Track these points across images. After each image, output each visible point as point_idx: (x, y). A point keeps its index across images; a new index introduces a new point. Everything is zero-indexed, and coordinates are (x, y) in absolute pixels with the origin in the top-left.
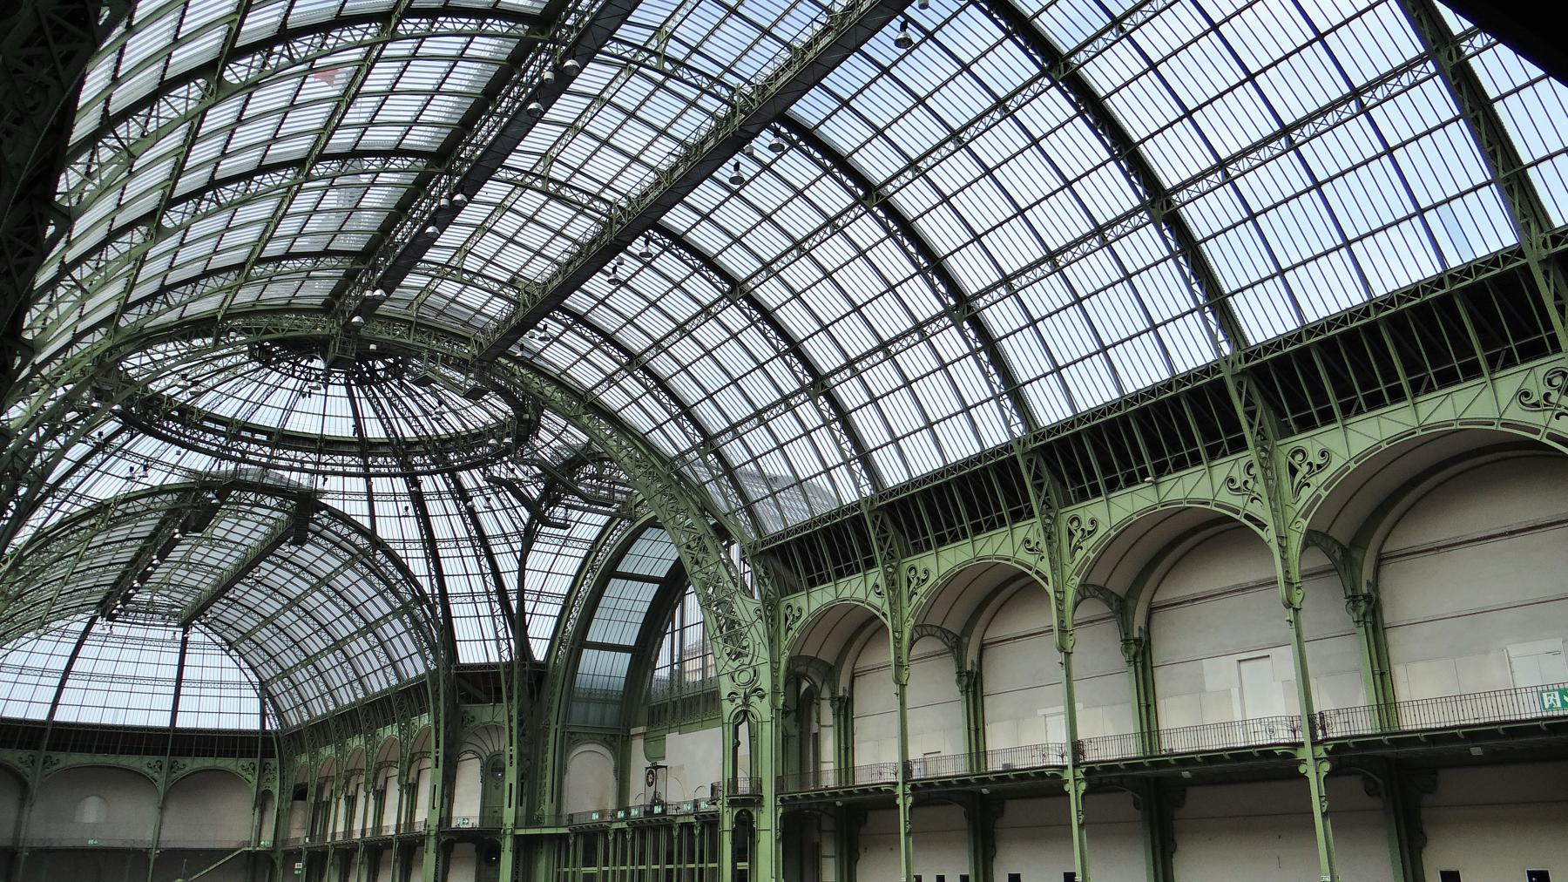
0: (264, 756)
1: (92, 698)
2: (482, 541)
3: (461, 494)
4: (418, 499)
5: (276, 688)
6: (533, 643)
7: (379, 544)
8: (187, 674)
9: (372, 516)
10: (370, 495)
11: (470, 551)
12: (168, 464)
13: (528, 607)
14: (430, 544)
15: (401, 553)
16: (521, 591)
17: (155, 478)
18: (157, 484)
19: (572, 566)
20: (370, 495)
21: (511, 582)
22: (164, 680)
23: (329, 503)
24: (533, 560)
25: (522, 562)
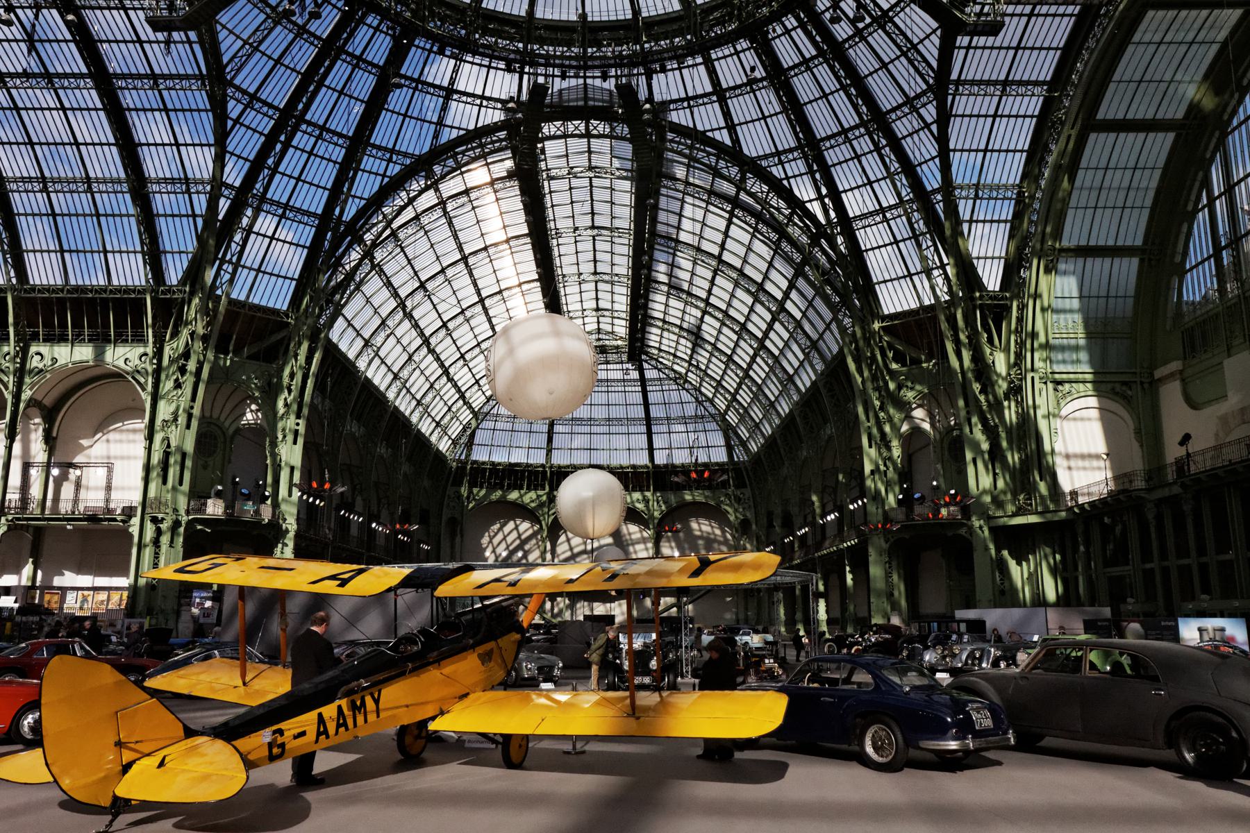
0: (737, 487)
1: (578, 441)
2: (877, 121)
3: (834, 53)
4: (778, 78)
5: (732, 418)
6: (980, 266)
7: (751, 166)
8: (655, 412)
9: (731, 127)
10: (720, 94)
11: (864, 144)
12: (473, 95)
13: (964, 209)
14: (811, 148)
15: (777, 172)
16: (948, 186)
17: (463, 116)
18: (471, 127)
19: (1020, 135)
20: (720, 94)
21: (931, 178)
22: (634, 419)
23: (674, 117)
24: (956, 130)
25: (942, 140)
